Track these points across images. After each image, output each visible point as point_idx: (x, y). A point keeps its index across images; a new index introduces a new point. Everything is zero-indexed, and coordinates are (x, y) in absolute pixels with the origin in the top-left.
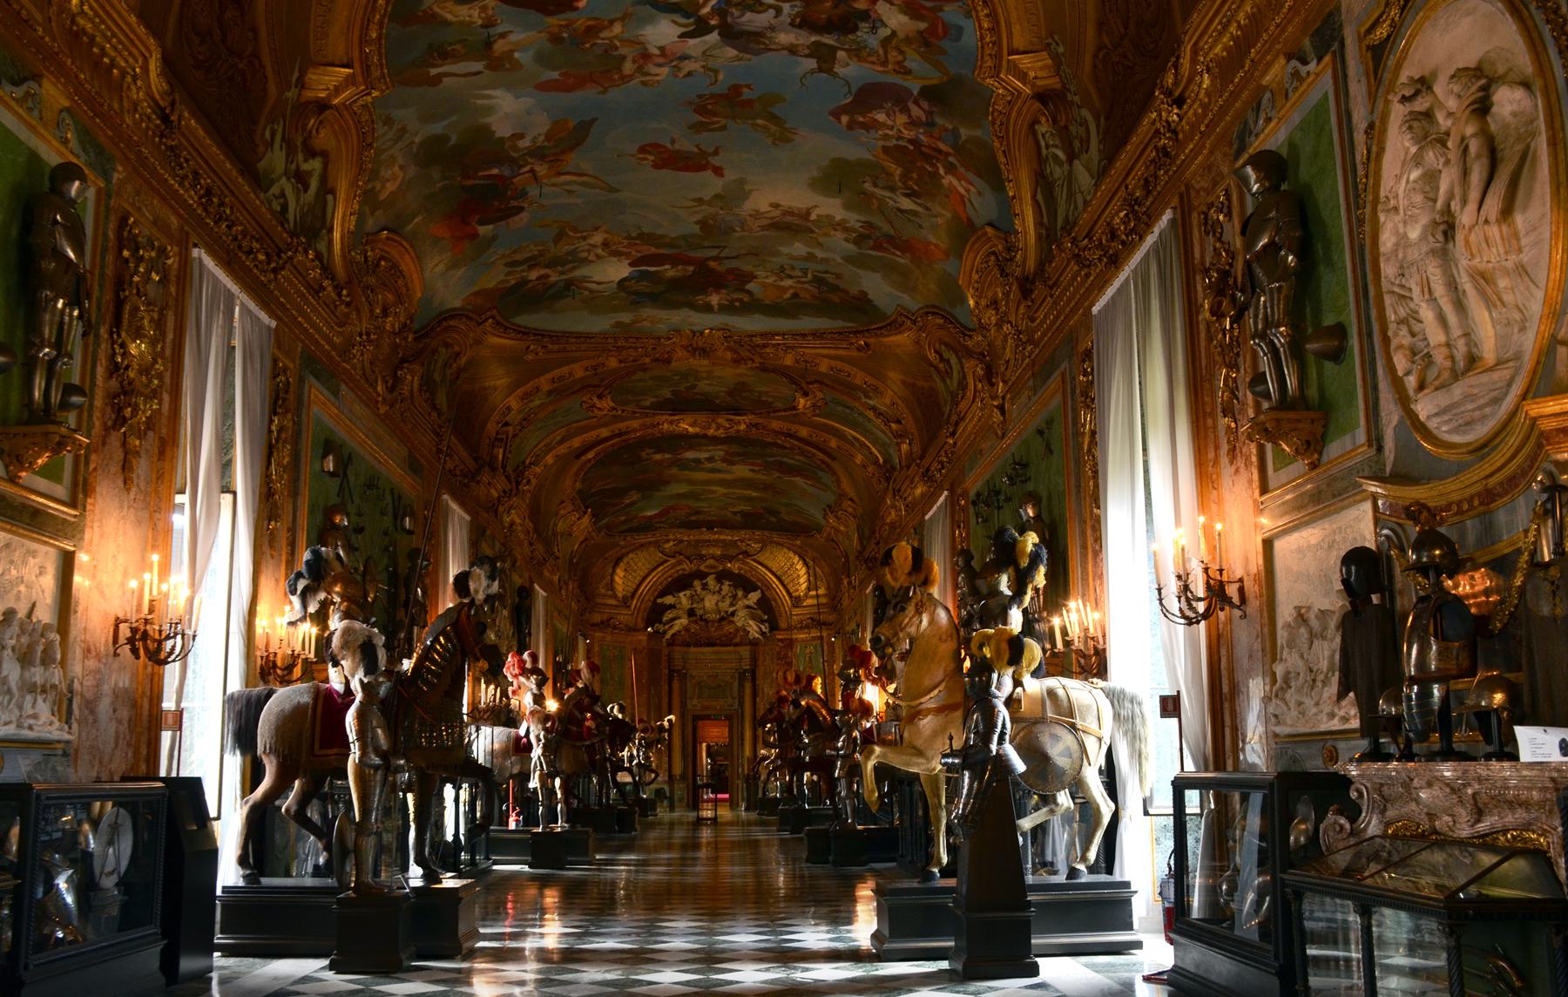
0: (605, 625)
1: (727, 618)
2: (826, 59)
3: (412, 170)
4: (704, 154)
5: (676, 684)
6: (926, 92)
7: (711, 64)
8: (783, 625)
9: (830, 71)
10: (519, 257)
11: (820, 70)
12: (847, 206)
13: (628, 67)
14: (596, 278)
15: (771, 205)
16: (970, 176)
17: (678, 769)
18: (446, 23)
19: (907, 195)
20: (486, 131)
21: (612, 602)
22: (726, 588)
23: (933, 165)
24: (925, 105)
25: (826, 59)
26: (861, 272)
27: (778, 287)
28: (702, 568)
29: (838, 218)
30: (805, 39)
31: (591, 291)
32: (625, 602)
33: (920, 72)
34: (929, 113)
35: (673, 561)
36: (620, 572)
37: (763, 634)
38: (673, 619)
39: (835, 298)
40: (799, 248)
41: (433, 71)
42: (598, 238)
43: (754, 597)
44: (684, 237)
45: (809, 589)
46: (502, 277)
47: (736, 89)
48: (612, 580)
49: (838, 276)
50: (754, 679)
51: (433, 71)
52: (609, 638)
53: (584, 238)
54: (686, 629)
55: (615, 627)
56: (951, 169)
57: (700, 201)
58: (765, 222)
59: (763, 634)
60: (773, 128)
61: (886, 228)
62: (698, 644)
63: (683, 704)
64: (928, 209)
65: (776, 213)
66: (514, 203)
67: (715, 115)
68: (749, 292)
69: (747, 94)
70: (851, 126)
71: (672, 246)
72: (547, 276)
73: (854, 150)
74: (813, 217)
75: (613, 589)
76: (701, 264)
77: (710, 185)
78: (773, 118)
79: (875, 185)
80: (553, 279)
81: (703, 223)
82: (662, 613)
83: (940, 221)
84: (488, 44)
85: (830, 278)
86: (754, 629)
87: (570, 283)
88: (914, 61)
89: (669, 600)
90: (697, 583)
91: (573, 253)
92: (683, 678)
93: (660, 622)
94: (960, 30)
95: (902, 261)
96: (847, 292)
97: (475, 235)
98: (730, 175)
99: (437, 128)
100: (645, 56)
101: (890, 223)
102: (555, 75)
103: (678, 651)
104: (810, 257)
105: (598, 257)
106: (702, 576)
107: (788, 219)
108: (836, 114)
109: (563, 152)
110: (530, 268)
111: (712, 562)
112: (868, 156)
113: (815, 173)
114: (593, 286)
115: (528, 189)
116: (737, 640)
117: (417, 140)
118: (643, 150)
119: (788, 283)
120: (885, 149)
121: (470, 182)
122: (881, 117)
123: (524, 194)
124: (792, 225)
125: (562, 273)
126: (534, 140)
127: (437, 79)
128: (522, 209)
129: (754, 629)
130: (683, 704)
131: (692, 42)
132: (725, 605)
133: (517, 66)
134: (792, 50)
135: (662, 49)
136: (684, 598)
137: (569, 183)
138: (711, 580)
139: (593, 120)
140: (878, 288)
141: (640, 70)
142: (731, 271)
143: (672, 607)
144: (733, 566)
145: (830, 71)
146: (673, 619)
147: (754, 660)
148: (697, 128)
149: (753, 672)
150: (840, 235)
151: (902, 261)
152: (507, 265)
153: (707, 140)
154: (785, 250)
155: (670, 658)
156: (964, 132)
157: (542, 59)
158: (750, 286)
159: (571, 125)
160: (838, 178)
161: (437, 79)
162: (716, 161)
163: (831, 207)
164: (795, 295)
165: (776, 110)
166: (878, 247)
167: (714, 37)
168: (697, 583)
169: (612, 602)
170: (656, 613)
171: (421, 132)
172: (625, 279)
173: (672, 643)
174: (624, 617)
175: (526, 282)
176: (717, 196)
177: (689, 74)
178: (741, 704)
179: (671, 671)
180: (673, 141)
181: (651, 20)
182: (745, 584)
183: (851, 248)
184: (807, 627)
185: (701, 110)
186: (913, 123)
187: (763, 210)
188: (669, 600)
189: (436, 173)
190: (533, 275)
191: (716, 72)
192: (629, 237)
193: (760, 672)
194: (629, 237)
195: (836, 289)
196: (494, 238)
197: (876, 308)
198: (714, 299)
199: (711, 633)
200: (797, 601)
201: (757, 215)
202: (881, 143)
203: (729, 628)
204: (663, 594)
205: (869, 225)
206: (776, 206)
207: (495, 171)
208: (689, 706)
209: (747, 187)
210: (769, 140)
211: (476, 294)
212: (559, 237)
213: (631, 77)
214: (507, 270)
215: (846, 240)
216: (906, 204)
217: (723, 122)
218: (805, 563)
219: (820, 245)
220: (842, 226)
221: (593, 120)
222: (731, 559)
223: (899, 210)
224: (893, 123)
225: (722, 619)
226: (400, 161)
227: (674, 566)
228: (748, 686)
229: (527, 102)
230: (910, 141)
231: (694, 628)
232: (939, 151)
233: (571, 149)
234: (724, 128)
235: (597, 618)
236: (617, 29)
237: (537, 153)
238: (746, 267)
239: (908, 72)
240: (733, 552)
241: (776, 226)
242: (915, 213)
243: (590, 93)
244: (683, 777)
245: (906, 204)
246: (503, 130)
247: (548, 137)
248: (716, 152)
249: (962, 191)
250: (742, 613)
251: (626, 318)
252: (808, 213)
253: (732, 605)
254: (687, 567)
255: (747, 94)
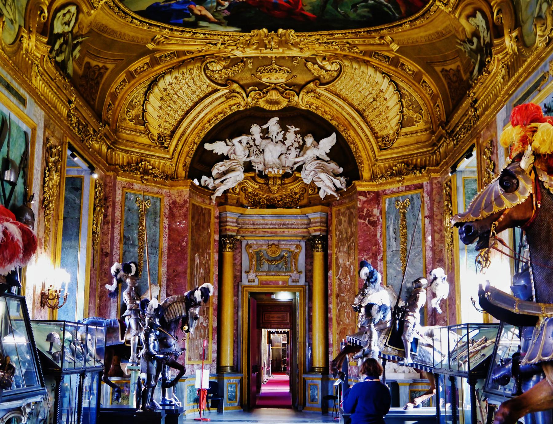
0: (130, 168)
1: (292, 174)
5: (228, 254)
8: (366, 174)
17: (228, 361)
21: (144, 140)
22: (291, 136)
28: (262, 104)
32: (161, 142)
35: (224, 91)
36: (154, 100)
37: (338, 190)
38: (225, 173)
43: (327, 143)
45: (402, 124)
48: (144, 111)
50: (325, 249)
52: (137, 186)
54: (242, 186)
55: (146, 172)
59: (338, 190)
62: (256, 204)
63: (237, 280)
75: (144, 123)
82: (212, 166)
86: (327, 185)
89: (219, 147)
90: (255, 129)
92: (237, 245)
93: (209, 175)
103: (232, 214)
106: (260, 116)
111: (274, 95)
116: (305, 201)
129: (327, 185)
130: (237, 280)
132: (291, 159)
136: (238, 148)
138: (273, 124)
143: (224, 158)
144: (302, 101)
146: (225, 173)
147: (327, 222)
149: (325, 240)
155: (222, 222)
168: (255, 129)
169: (144, 140)
170: (202, 163)
173: (224, 200)
174: (160, 160)
178: (309, 279)
179: (223, 236)
182: (315, 126)
184: (400, 173)
188: (219, 147)
193: (333, 241)
199: (273, 190)
200: (385, 143)
203: (295, 187)
204: (212, 137)
208: (245, 282)
218: (398, 89)
222: (299, 88)
225: (286, 175)
227: (228, 97)
228: (318, 256)
231: (252, 186)
235: (121, 157)
240: (301, 79)
244: (235, 369)
250: (310, 167)
253: (297, 156)
254: (242, 102)
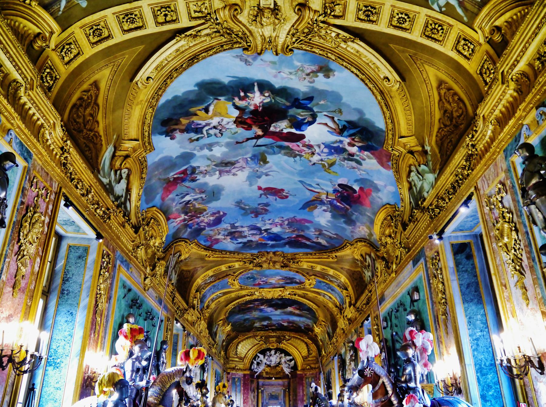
2: (233, 226)
3: (358, 224)
4: (265, 194)
6: (204, 229)
7: (263, 222)
9: (231, 224)
10: (354, 164)
11: (234, 224)
12: (206, 184)
13: (286, 222)
14: (327, 129)
15: (237, 175)
16: (179, 225)
18: (326, 241)
19: (190, 201)
20: (333, 216)
23: (190, 216)
24: (202, 227)
25: (233, 226)
26: (182, 150)
27: (220, 115)
29: (207, 176)
30: (240, 229)
31: (332, 118)
33: (208, 231)
34: (200, 226)
39: (184, 121)
40: (218, 152)
41: (335, 236)
42: (315, 158)
44: (274, 153)
46: (368, 160)
47: (256, 216)
49: (191, 141)
51: (335, 236)
53: (322, 160)
56: (185, 220)
57: (267, 175)
58: (237, 165)
60: (243, 206)
61: (187, 184)
64: (180, 203)
65: (234, 171)
66: (340, 190)
67: (262, 209)
68: (237, 107)
69: (253, 215)
70: (219, 212)
71: (281, 147)
72: (350, 144)
73: (214, 205)
74: (217, 173)
76: (267, 133)
77: (264, 182)
78: (244, 209)
79: (201, 197)
80: (347, 140)
81: (265, 162)
83: (174, 204)
84: (319, 234)
85: (194, 136)
87: (341, 132)
88: (212, 233)
91: (330, 154)
94: (205, 242)
95: (172, 174)
96: (182, 131)
97: (361, 189)
98: (255, 187)
99: (344, 225)
100: (281, 225)
101: (188, 187)
102: (306, 224)
104: (210, 147)
105: (319, 146)
107: (228, 169)
108: (225, 214)
109: (314, 200)
110: (352, 155)
112: (208, 205)
113: (223, 192)
114: (331, 124)
115: (332, 192)
117: (351, 228)
118: (287, 197)
119: (215, 121)
120: (205, 210)
121: (348, 207)
122: (212, 218)
123: (335, 191)
124: (225, 165)
125: (341, 142)
126: (321, 207)
127: (335, 234)
128: (340, 185)
131: (269, 228)
133: (315, 229)
134: (242, 227)
135: (276, 226)
137: (317, 188)
139: (300, 209)
140: (168, 147)
141: (283, 221)
142: (249, 128)
145: (231, 224)
148: (267, 205)
150: (202, 169)
151: (172, 174)
152: (360, 164)
153: (264, 200)
154: (224, 149)
156: (189, 230)
157: (308, 228)
158: (236, 113)
159: (308, 209)
160: (215, 194)
161: (335, 234)
162: (261, 192)
163: (212, 180)
164: (207, 110)
165: (243, 212)
166: (184, 172)
167: (263, 229)
171: (349, 228)
172: (310, 123)
175: (361, 149)
176: (259, 177)
177: (269, 220)
180: (276, 199)
181: (279, 232)
183: (194, 164)
185: (266, 210)
186: (202, 221)
187: (240, 171)
189: (354, 217)
190: (354, 150)
191: (262, 220)
192: (301, 156)
194: (301, 156)
195: (187, 130)
196: (356, 181)
197: (161, 134)
198: (257, 99)
201: (242, 168)
202: (208, 211)
205: (194, 180)
206: (234, 175)
207: (338, 204)
209: (248, 182)
210: (243, 201)
211: (382, 165)
212: (332, 165)
213: (286, 220)
214: (362, 162)
215: (199, 167)
216: (187, 198)
217: (259, 206)
219: (208, 159)
220: (205, 173)
221: (300, 209)
223: (188, 194)
224: (206, 218)
226: (358, 229)
229: (317, 219)
230: (200, 217)
232: (191, 220)
233: (311, 201)
234: (259, 204)
236: (287, 231)
237: (322, 203)
238: (240, 130)
239: (211, 230)
241: (232, 164)
242: (183, 198)
243: (299, 217)
245: (187, 198)
246: (328, 215)
247: (316, 207)
248: (261, 195)
249: (178, 219)
251: (321, 82)
252: (220, 174)
255: (253, 215)
